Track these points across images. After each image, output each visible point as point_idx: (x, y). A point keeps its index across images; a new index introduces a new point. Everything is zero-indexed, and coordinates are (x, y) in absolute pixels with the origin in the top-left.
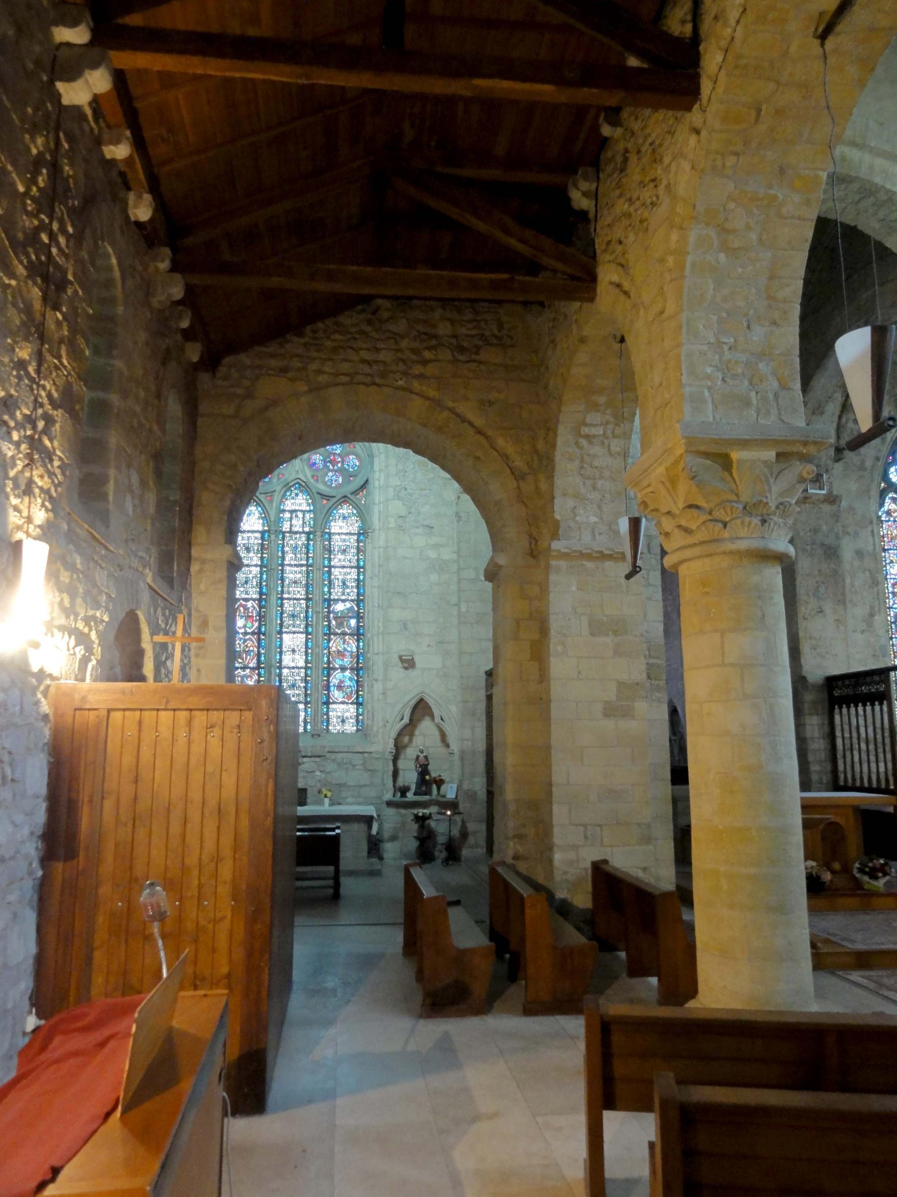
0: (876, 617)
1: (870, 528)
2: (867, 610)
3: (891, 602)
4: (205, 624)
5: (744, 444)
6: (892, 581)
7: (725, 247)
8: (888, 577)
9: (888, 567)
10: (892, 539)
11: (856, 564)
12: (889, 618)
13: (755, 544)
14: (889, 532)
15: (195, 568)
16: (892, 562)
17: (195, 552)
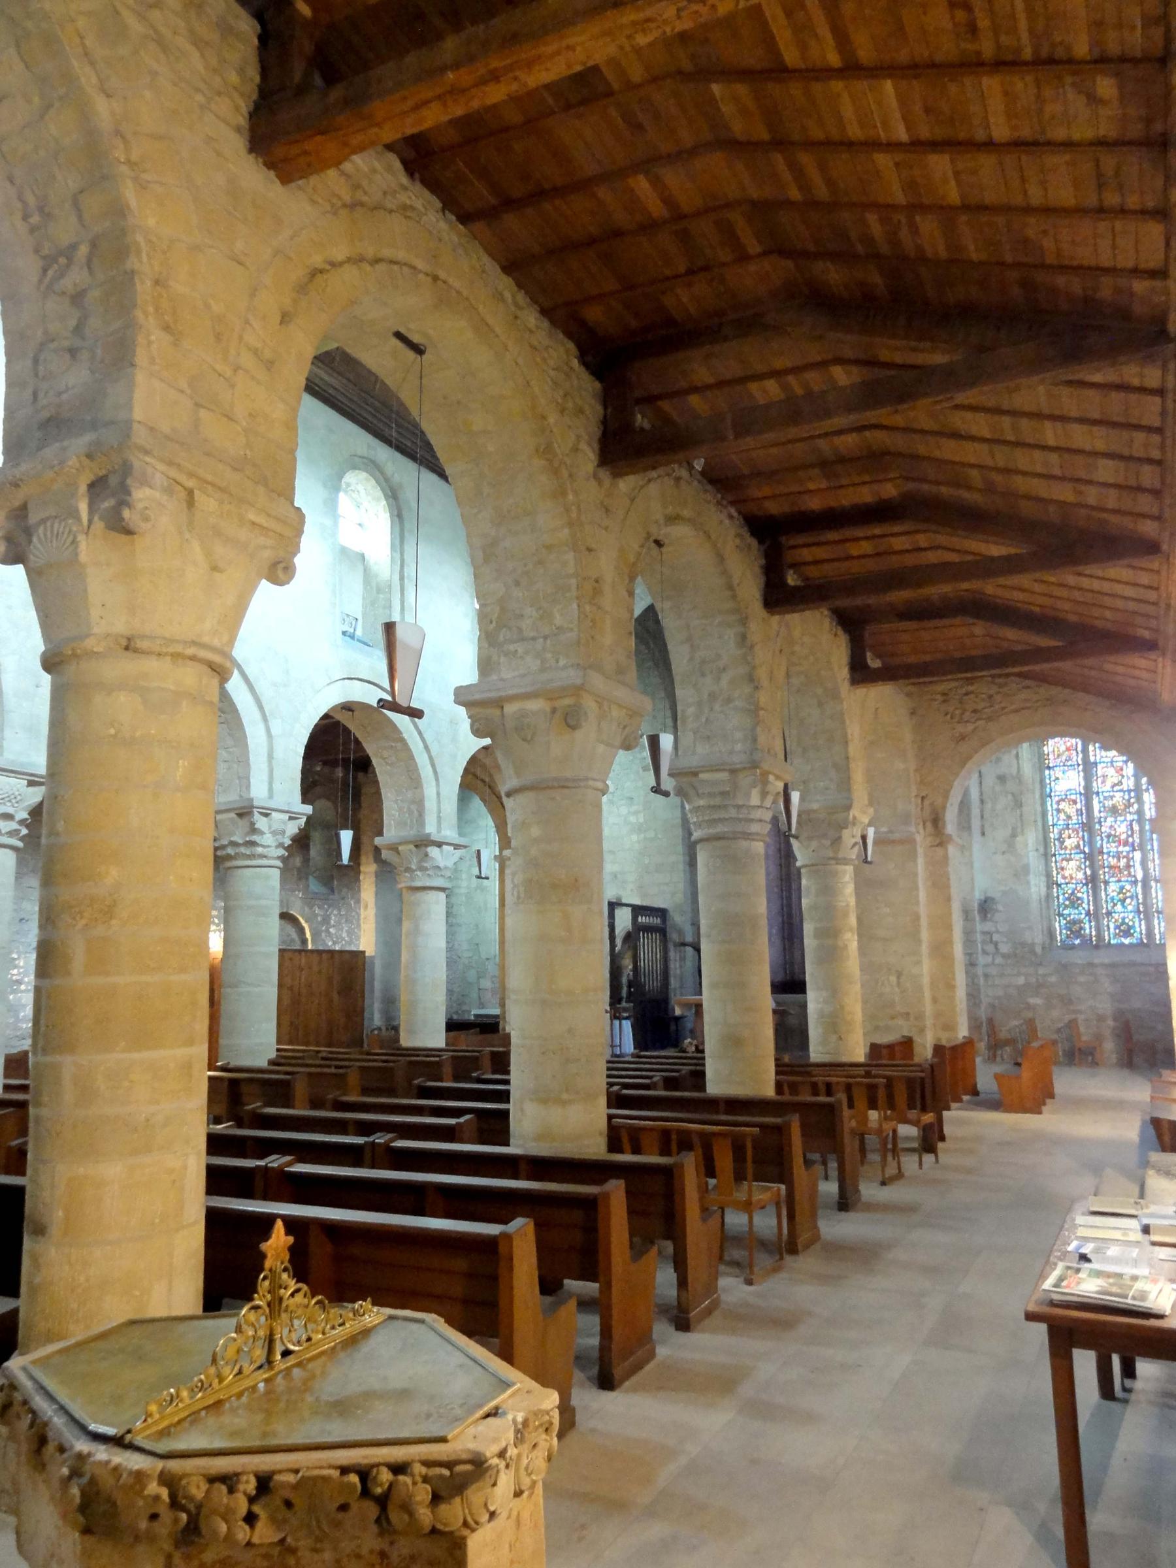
0: (1019, 839)
1: (1014, 752)
2: (1009, 831)
3: (1055, 819)
4: (366, 907)
5: (400, 844)
6: (1057, 798)
7: (387, 763)
8: (1053, 794)
9: (1053, 784)
10: (1059, 756)
11: (998, 788)
12: (1052, 835)
13: (408, 884)
14: (1056, 749)
15: (362, 877)
16: (1057, 779)
17: (362, 869)
